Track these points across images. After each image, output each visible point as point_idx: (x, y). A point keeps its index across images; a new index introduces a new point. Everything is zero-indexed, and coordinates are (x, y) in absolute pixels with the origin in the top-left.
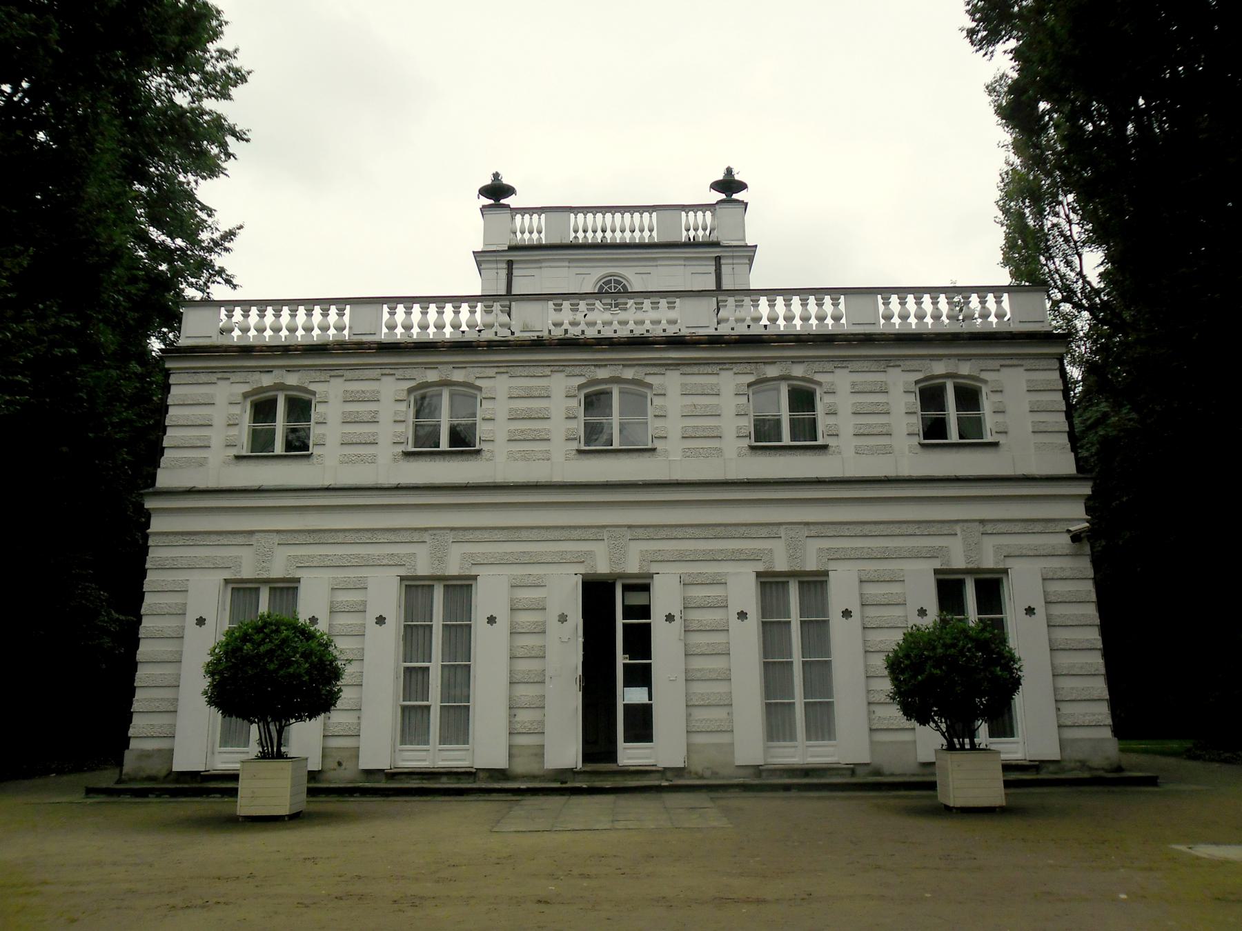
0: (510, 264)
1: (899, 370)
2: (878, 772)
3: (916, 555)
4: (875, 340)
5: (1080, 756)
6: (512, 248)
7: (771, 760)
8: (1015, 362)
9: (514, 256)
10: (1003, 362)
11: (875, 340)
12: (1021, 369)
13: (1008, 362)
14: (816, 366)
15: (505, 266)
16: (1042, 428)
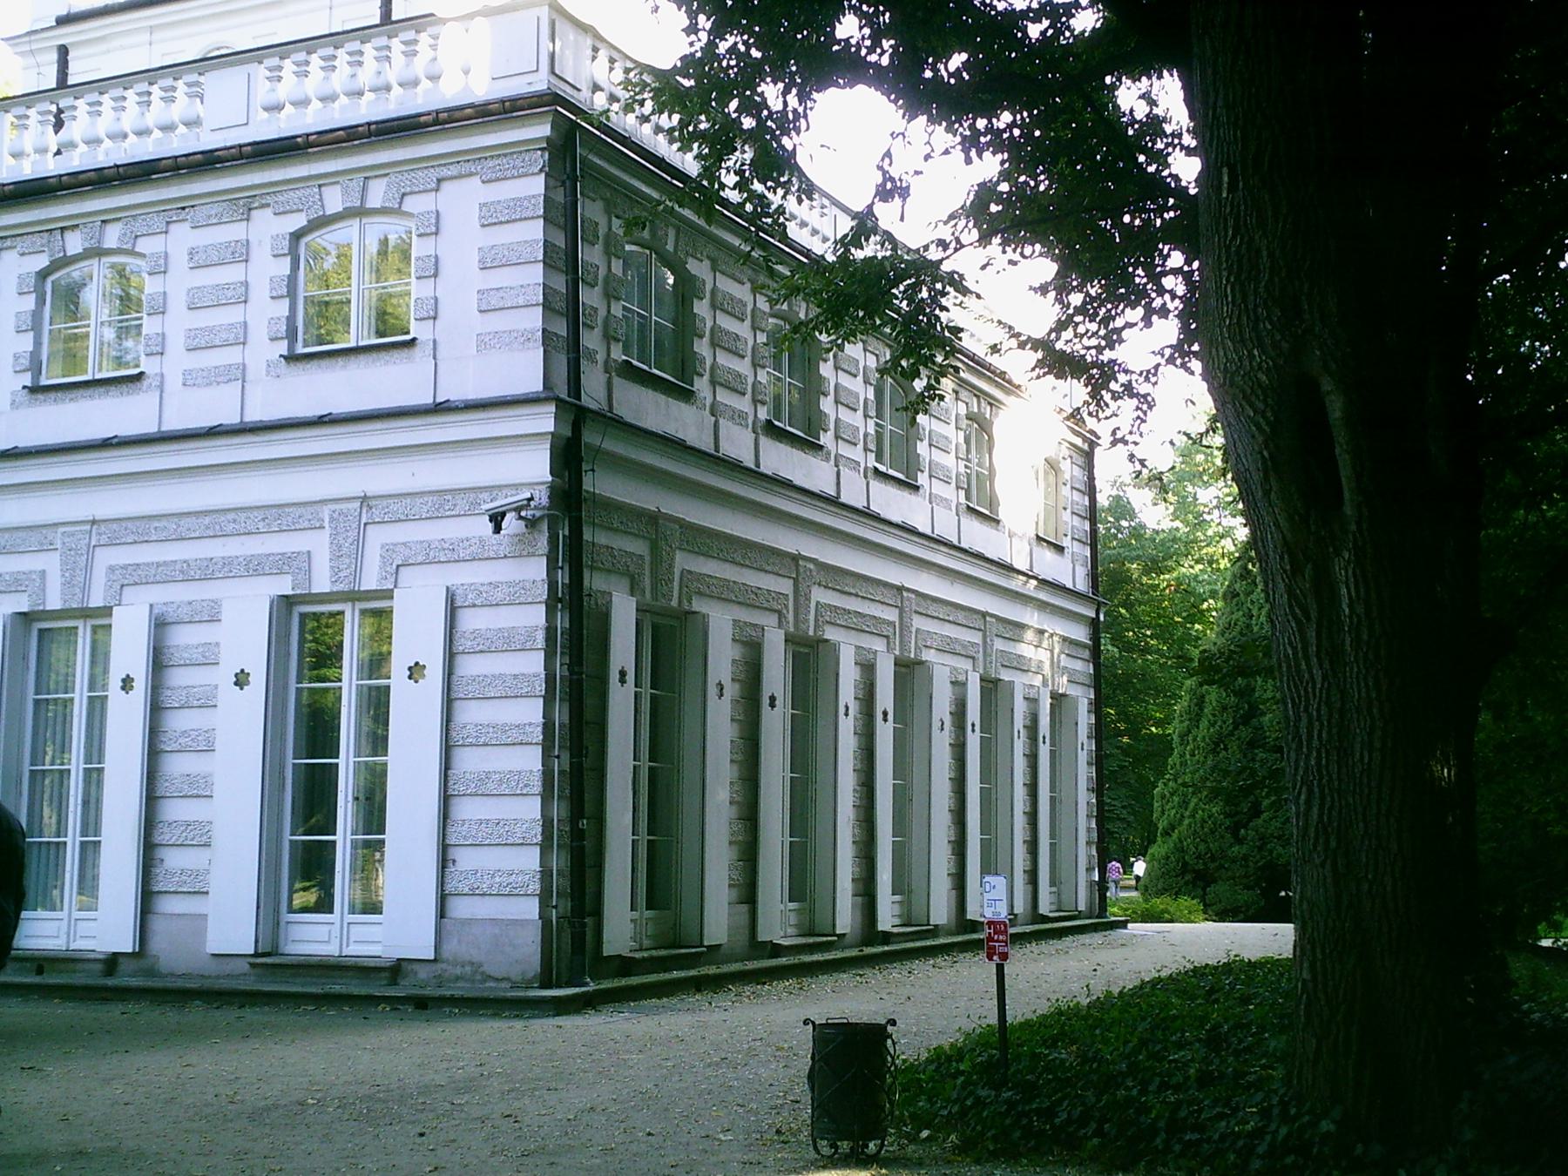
0: (63, 51)
1: (268, 212)
2: (151, 972)
3: (255, 568)
4: (221, 160)
5: (476, 956)
6: (63, 21)
7: (353, 950)
8: (465, 168)
9: (68, 35)
10: (445, 172)
11: (221, 160)
12: (476, 180)
13: (453, 170)
14: (139, 227)
15: (54, 56)
16: (495, 303)
